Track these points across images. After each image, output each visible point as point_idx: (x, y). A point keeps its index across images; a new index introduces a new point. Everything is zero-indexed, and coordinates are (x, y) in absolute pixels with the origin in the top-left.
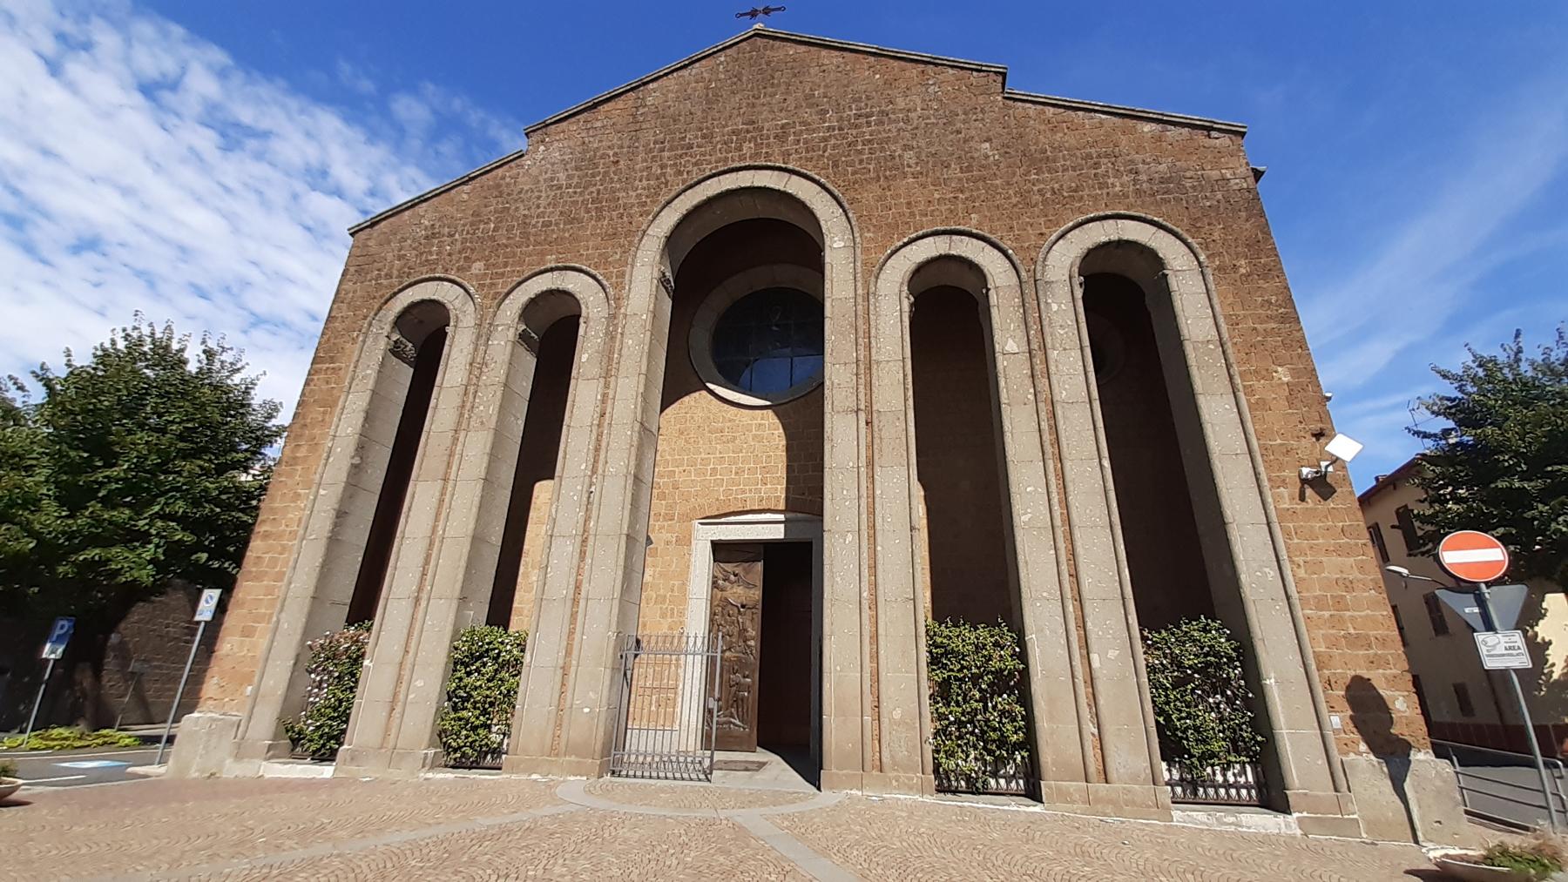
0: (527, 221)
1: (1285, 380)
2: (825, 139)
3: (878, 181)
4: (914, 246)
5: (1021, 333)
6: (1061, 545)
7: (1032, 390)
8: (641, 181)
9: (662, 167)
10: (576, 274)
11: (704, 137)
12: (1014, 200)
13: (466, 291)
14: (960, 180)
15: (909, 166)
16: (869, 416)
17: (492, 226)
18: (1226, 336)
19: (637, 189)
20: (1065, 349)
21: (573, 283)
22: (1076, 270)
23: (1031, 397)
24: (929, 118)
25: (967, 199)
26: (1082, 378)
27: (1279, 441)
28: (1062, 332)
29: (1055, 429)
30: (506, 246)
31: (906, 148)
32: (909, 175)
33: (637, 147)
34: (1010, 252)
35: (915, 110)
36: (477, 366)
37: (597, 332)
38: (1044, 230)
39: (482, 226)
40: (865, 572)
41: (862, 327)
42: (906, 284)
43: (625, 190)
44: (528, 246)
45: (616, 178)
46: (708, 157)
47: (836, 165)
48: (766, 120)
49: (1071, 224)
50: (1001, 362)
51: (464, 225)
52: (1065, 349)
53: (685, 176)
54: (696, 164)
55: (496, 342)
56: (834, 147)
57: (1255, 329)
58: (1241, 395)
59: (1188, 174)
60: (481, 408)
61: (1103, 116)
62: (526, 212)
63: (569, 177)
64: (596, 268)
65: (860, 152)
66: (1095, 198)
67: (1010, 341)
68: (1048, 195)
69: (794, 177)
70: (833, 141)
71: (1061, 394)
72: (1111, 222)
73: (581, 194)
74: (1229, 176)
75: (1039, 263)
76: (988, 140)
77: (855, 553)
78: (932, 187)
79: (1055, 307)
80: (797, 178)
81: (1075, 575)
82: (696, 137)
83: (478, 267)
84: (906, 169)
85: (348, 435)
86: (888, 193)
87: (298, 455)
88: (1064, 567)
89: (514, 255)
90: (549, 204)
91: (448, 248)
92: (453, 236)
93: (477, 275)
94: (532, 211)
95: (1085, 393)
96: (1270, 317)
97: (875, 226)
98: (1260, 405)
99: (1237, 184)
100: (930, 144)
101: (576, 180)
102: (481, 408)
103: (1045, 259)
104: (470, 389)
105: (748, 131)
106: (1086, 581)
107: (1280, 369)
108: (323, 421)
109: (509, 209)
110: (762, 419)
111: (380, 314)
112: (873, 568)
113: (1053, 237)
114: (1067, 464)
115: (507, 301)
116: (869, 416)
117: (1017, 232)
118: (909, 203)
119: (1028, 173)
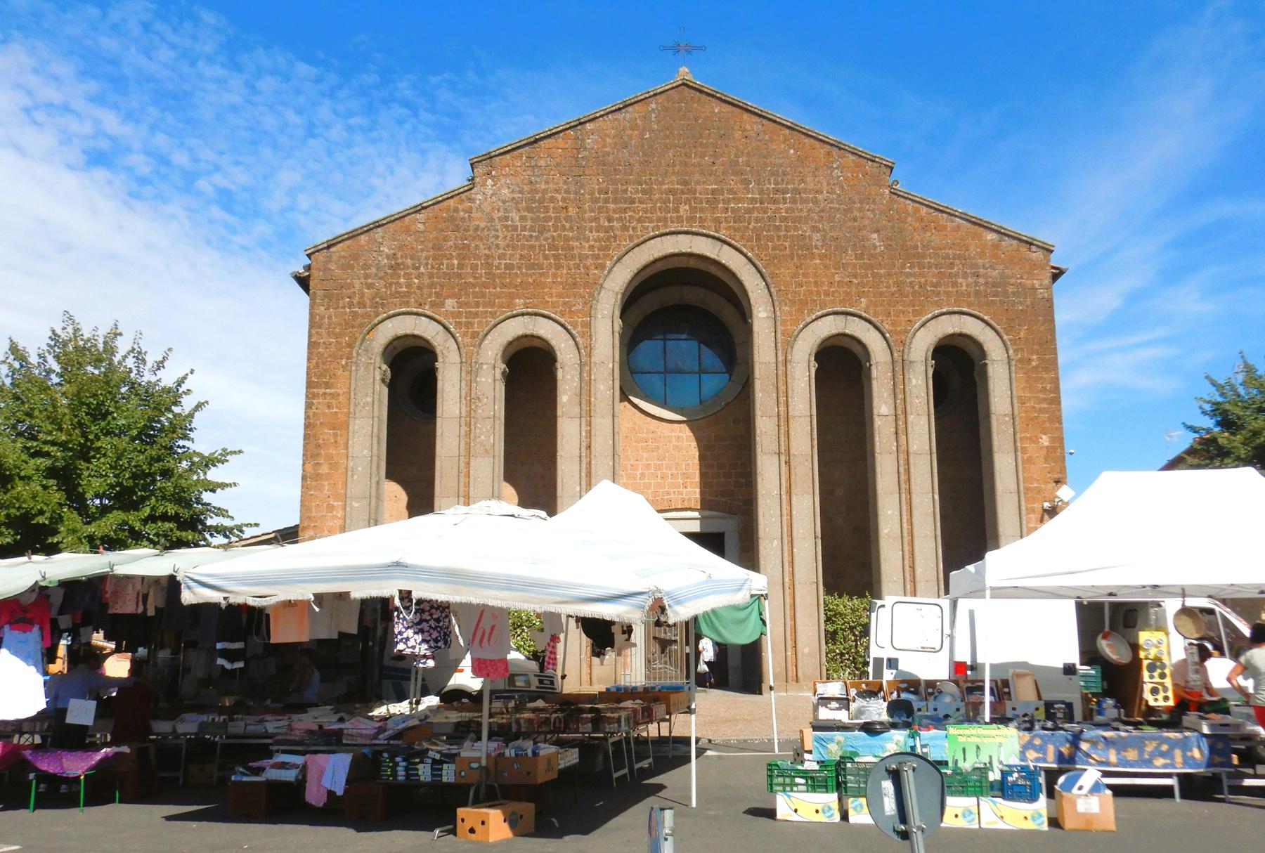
0: (490, 261)
1: (1046, 444)
2: (749, 211)
3: (792, 259)
4: (819, 322)
5: (891, 401)
6: (907, 549)
7: (895, 444)
8: (592, 232)
9: (610, 220)
10: (546, 320)
11: (644, 192)
12: (894, 289)
13: (445, 327)
14: (854, 265)
15: (817, 248)
16: (785, 454)
17: (456, 262)
18: (1016, 412)
19: (588, 241)
20: (918, 415)
21: (545, 330)
22: (930, 354)
23: (894, 448)
24: (832, 202)
25: (859, 284)
26: (927, 437)
27: (1036, 485)
28: (917, 401)
29: (908, 471)
30: (474, 286)
31: (815, 229)
32: (817, 257)
33: (583, 194)
34: (888, 335)
35: (822, 193)
36: (470, 399)
37: (572, 378)
38: (911, 318)
39: (445, 262)
40: (786, 564)
41: (782, 388)
42: (813, 355)
43: (578, 239)
44: (495, 288)
45: (567, 225)
46: (649, 215)
47: (758, 239)
48: (698, 183)
49: (930, 316)
50: (878, 422)
51: (427, 258)
52: (918, 415)
53: (631, 232)
54: (639, 221)
55: (483, 380)
56: (757, 221)
57: (1034, 407)
58: (1019, 454)
59: (1012, 281)
60: (483, 437)
61: (961, 221)
62: (487, 252)
63: (523, 218)
64: (562, 315)
65: (778, 228)
66: (948, 294)
67: (884, 406)
68: (916, 288)
69: (726, 247)
70: (756, 214)
71: (914, 447)
72: (957, 316)
73: (537, 238)
74: (1037, 286)
75: (907, 347)
76: (877, 231)
77: (779, 553)
78: (833, 271)
79: (914, 381)
80: (728, 248)
81: (913, 567)
82: (637, 192)
83: (450, 304)
84: (815, 251)
85: (365, 456)
86: (801, 272)
87: (320, 472)
88: (907, 562)
89: (484, 295)
90: (508, 246)
91: (416, 281)
92: (418, 268)
93: (452, 313)
94: (493, 251)
95: (928, 448)
96: (1044, 400)
97: (790, 300)
98: (1030, 460)
99: (1041, 293)
100: (832, 228)
101: (529, 223)
102: (483, 437)
103: (910, 343)
104: (469, 421)
105: (683, 192)
106: (919, 571)
107: (1044, 436)
108: (336, 442)
109: (469, 246)
110: (680, 432)
111: (364, 344)
112: (792, 562)
113: (917, 326)
114: (914, 497)
115: (486, 342)
116: (785, 454)
117: (893, 318)
118: (816, 283)
119: (903, 266)
